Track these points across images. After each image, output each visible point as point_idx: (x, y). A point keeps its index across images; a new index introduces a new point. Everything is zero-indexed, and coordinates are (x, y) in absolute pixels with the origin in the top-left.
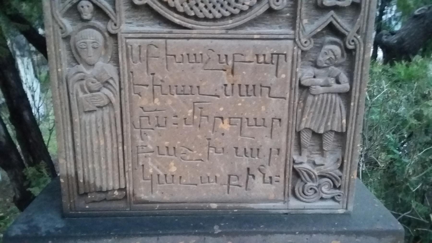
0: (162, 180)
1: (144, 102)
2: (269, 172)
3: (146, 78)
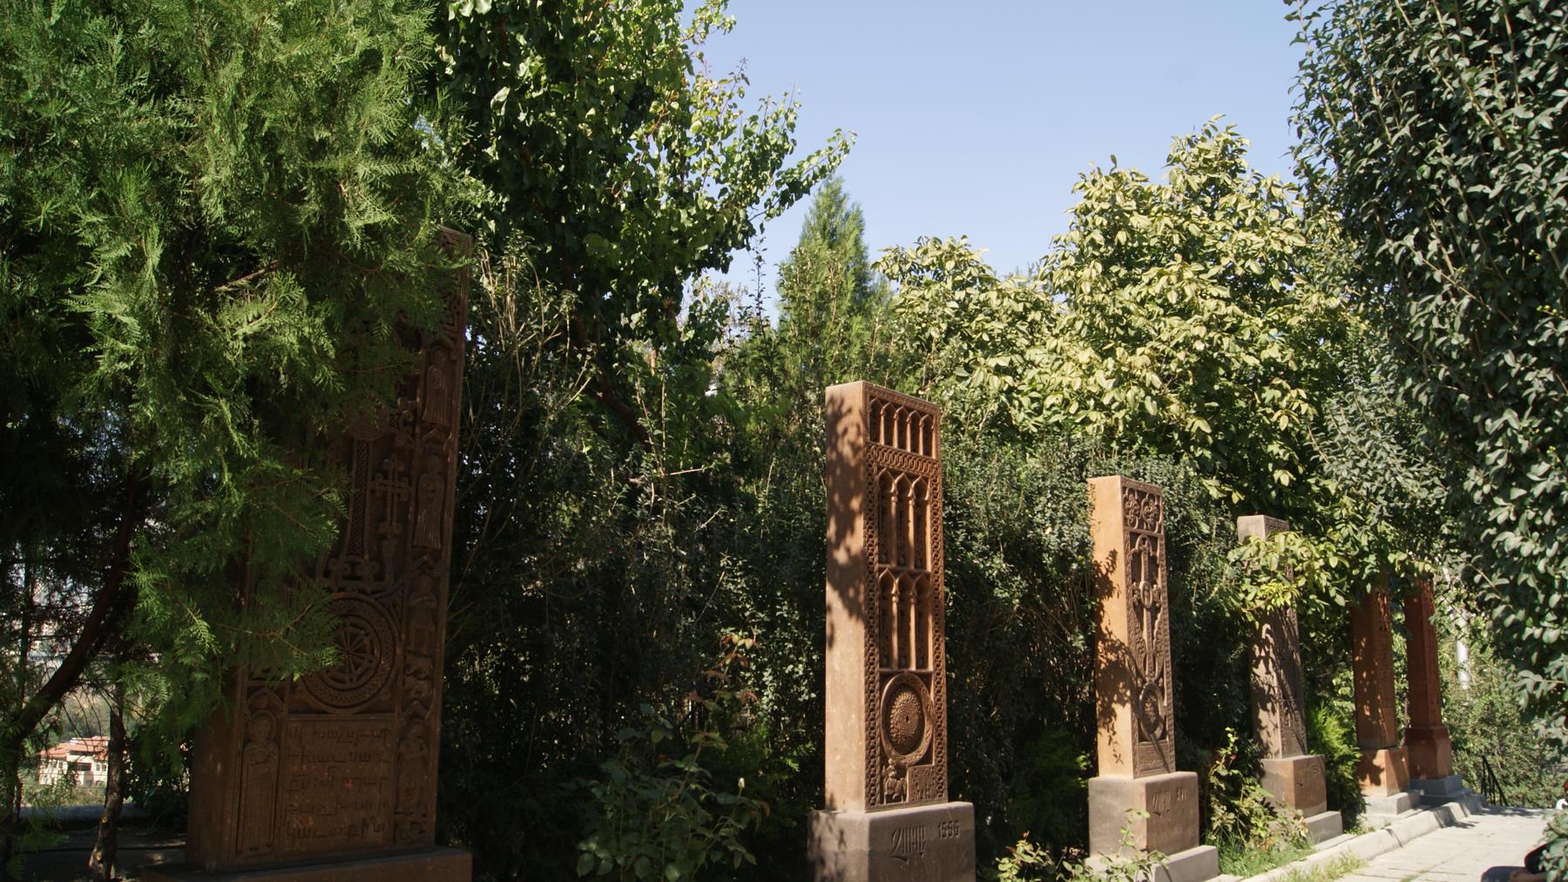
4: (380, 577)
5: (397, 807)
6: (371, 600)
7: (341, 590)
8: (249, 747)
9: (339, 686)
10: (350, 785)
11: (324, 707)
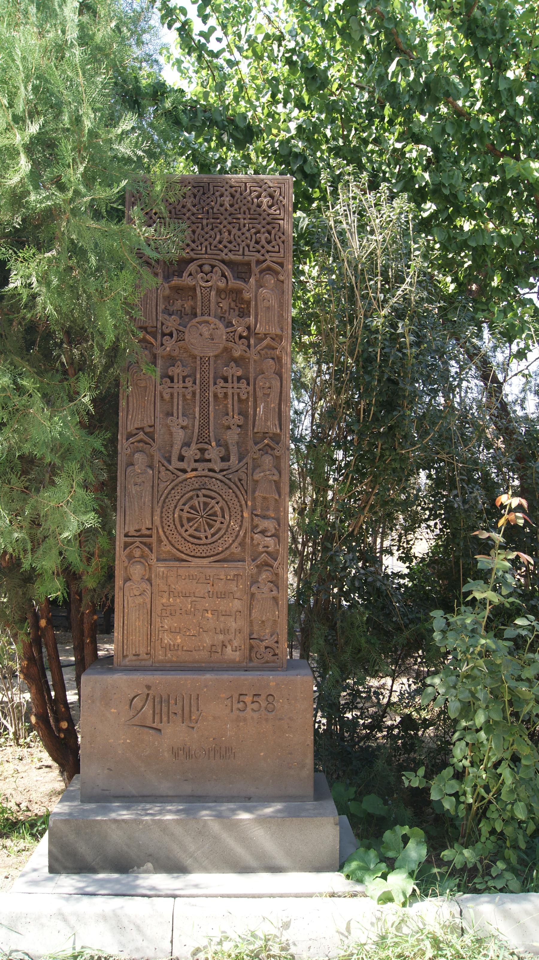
0: (172, 648)
1: (164, 600)
2: (236, 643)
3: (166, 588)
4: (225, 459)
5: (251, 633)
6: (219, 476)
7: (196, 470)
8: (128, 584)
9: (196, 541)
10: (209, 615)
11: (185, 557)
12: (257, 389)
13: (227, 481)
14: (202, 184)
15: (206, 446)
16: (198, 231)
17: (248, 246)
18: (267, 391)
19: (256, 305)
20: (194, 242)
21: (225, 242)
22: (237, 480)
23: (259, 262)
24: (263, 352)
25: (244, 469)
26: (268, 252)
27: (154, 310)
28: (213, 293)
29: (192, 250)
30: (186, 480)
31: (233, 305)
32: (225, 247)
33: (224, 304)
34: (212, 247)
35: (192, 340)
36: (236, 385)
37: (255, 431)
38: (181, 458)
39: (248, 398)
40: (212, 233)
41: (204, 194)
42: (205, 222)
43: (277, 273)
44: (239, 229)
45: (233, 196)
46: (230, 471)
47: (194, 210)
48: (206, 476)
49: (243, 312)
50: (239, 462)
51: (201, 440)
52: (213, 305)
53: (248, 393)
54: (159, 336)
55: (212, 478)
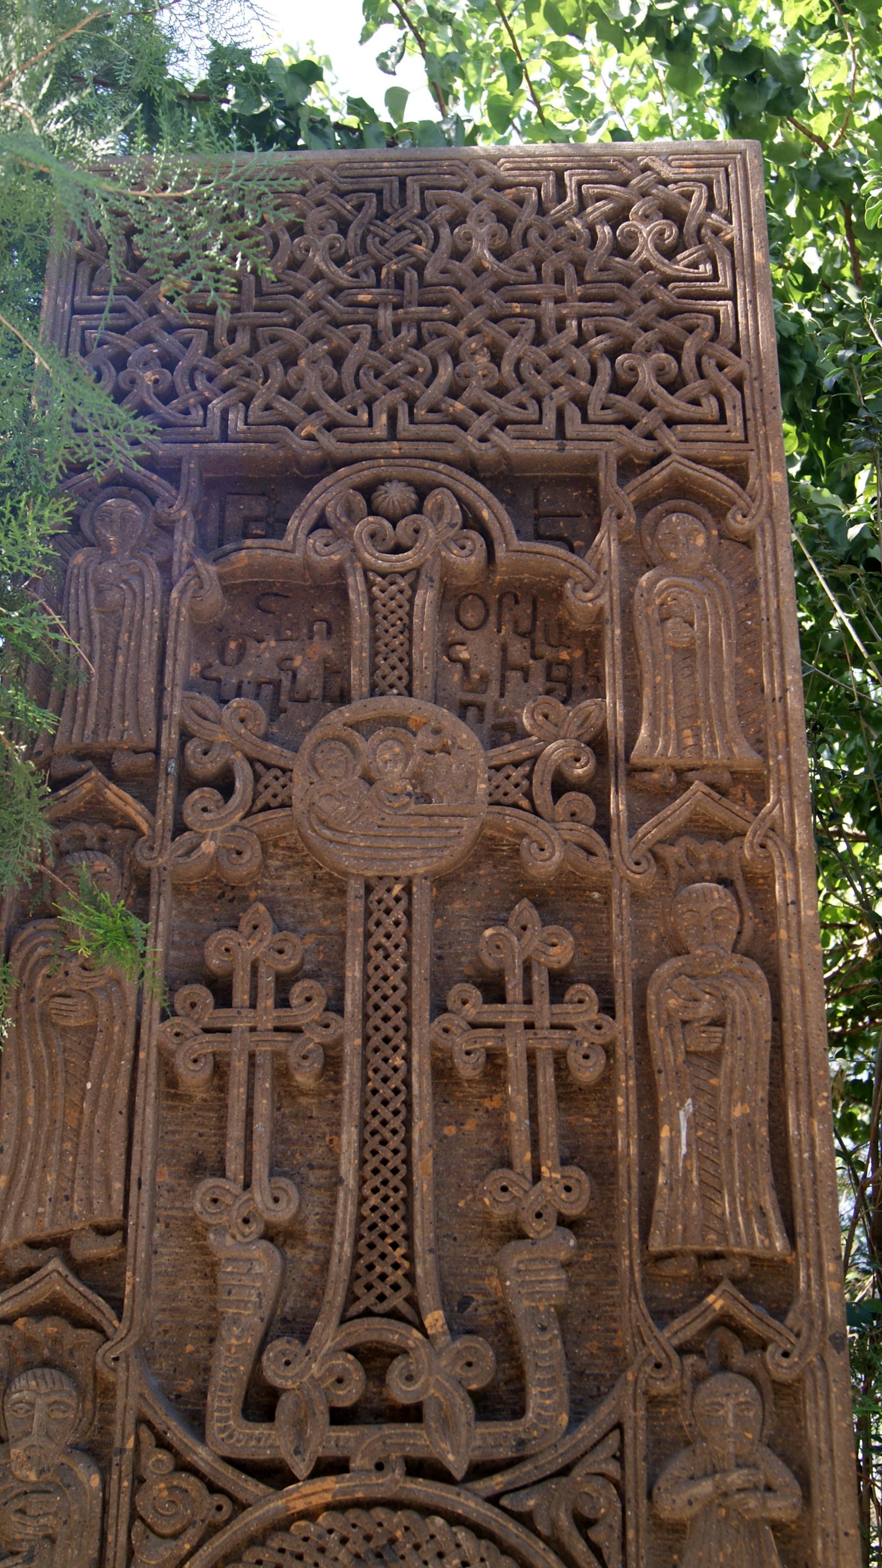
4: (497, 1402)
6: (468, 1503)
12: (657, 1032)
13: (512, 1531)
14: (373, 183)
15: (393, 1334)
16: (358, 352)
17: (581, 403)
18: (702, 1040)
19: (630, 642)
20: (337, 394)
21: (475, 391)
22: (565, 1521)
23: (628, 468)
24: (672, 853)
25: (602, 1461)
26: (671, 422)
27: (149, 675)
28: (426, 598)
29: (330, 427)
30: (283, 1525)
31: (518, 650)
32: (479, 410)
33: (478, 651)
34: (421, 413)
35: (325, 804)
36: (544, 1011)
37: (657, 1244)
38: (261, 1403)
39: (607, 1079)
40: (421, 359)
41: (382, 216)
42: (385, 317)
43: (718, 509)
44: (539, 340)
45: (504, 219)
46: (526, 1472)
47: (342, 276)
48: (394, 1505)
49: (567, 682)
50: (577, 1417)
51: (367, 1300)
52: (424, 653)
53: (609, 1050)
54: (167, 791)
55: (427, 1511)
